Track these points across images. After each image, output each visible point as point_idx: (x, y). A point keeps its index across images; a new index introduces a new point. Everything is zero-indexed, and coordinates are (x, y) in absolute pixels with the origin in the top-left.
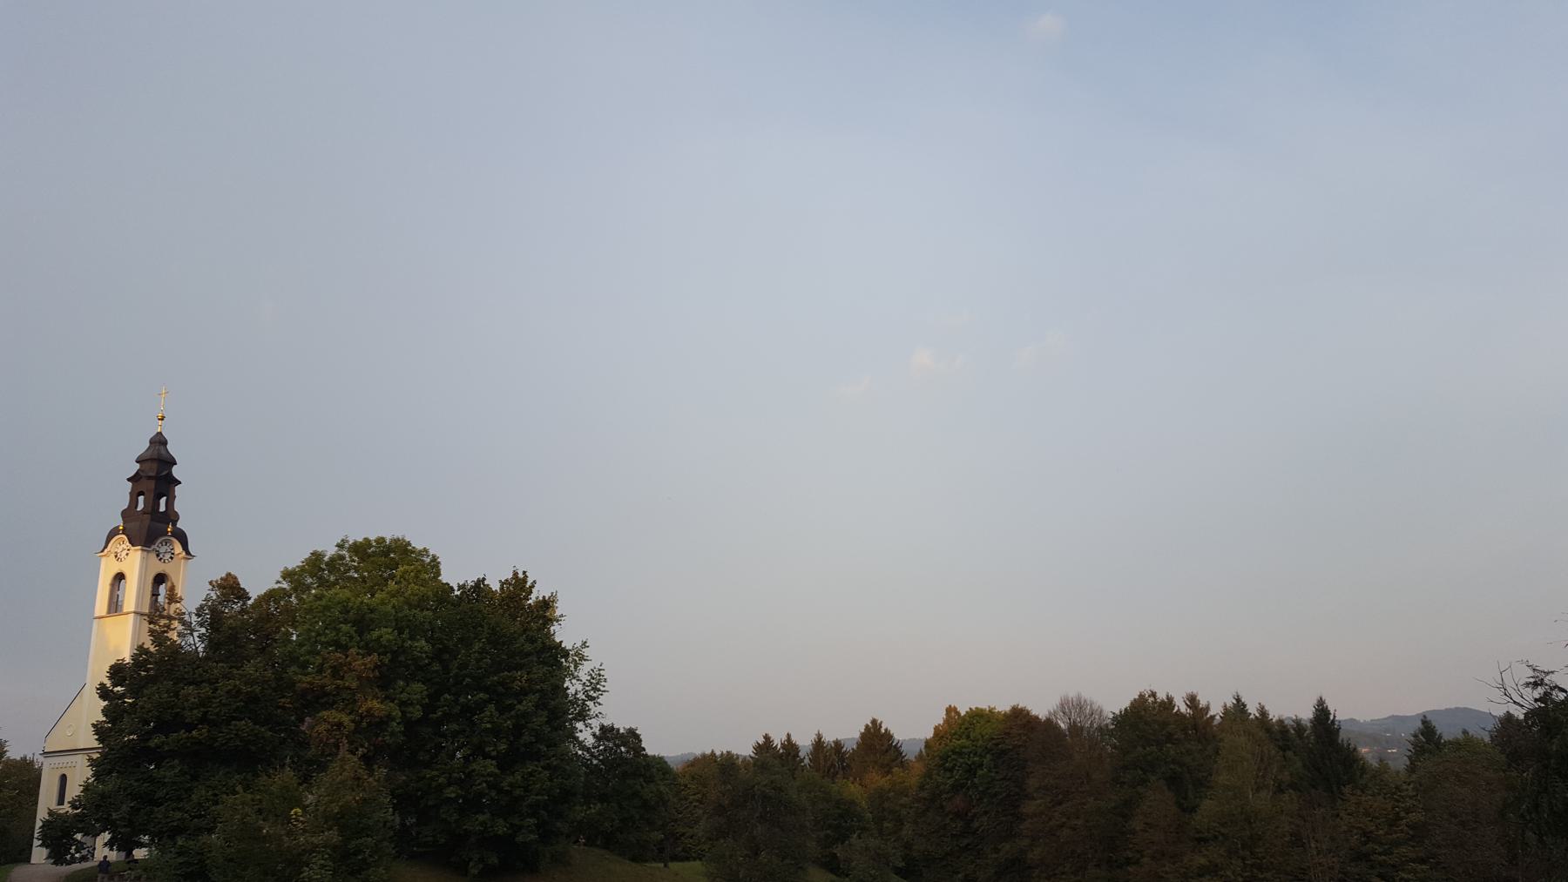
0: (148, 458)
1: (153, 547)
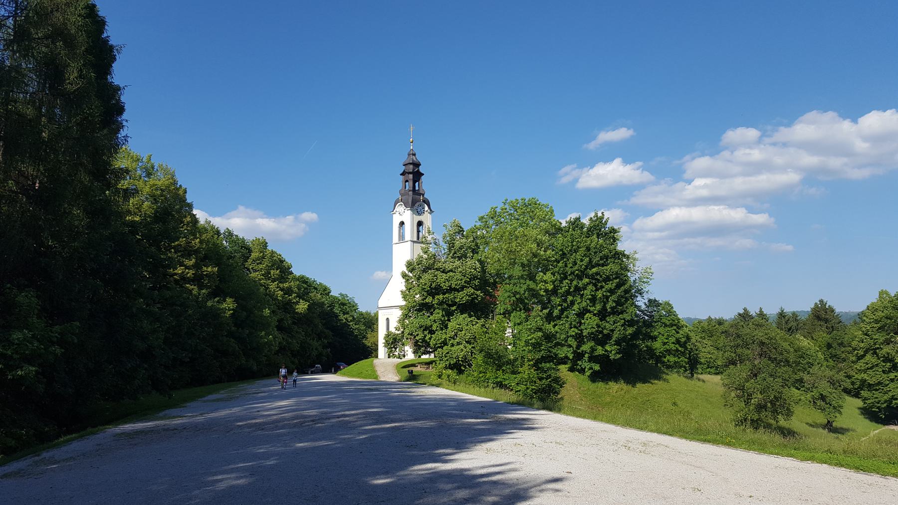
1: (415, 208)
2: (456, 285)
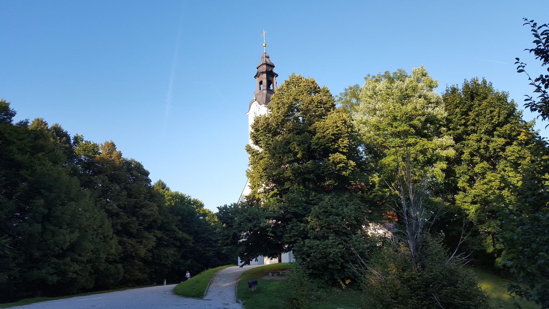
0: (262, 63)
2: (316, 144)
